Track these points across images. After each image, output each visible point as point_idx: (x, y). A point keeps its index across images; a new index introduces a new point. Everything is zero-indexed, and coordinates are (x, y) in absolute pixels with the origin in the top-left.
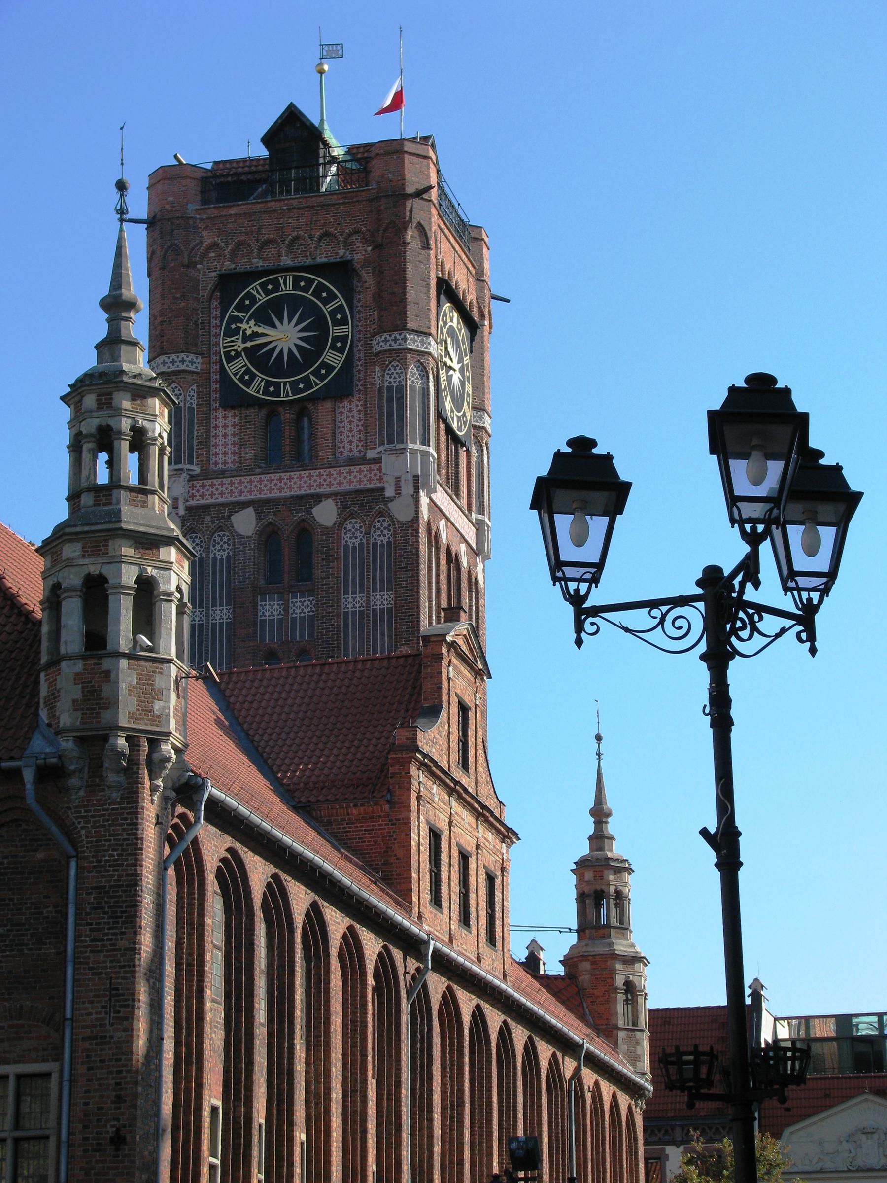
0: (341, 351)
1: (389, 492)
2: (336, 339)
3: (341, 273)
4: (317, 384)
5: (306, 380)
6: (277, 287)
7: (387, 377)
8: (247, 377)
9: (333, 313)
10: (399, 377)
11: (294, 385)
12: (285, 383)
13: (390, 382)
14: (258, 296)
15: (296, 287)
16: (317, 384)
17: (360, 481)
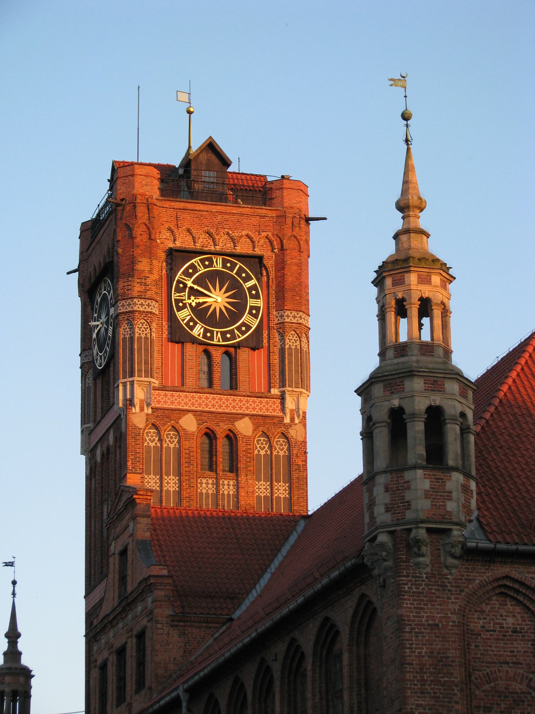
0: (256, 316)
1: (287, 420)
2: (252, 308)
3: (256, 262)
4: (239, 337)
5: (232, 332)
6: (211, 264)
7: (287, 341)
8: (191, 324)
9: (250, 289)
10: (296, 343)
11: (223, 334)
12: (217, 332)
13: (290, 345)
14: (198, 267)
15: (224, 266)
16: (239, 337)
17: (267, 410)
